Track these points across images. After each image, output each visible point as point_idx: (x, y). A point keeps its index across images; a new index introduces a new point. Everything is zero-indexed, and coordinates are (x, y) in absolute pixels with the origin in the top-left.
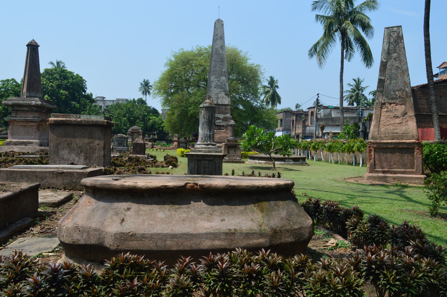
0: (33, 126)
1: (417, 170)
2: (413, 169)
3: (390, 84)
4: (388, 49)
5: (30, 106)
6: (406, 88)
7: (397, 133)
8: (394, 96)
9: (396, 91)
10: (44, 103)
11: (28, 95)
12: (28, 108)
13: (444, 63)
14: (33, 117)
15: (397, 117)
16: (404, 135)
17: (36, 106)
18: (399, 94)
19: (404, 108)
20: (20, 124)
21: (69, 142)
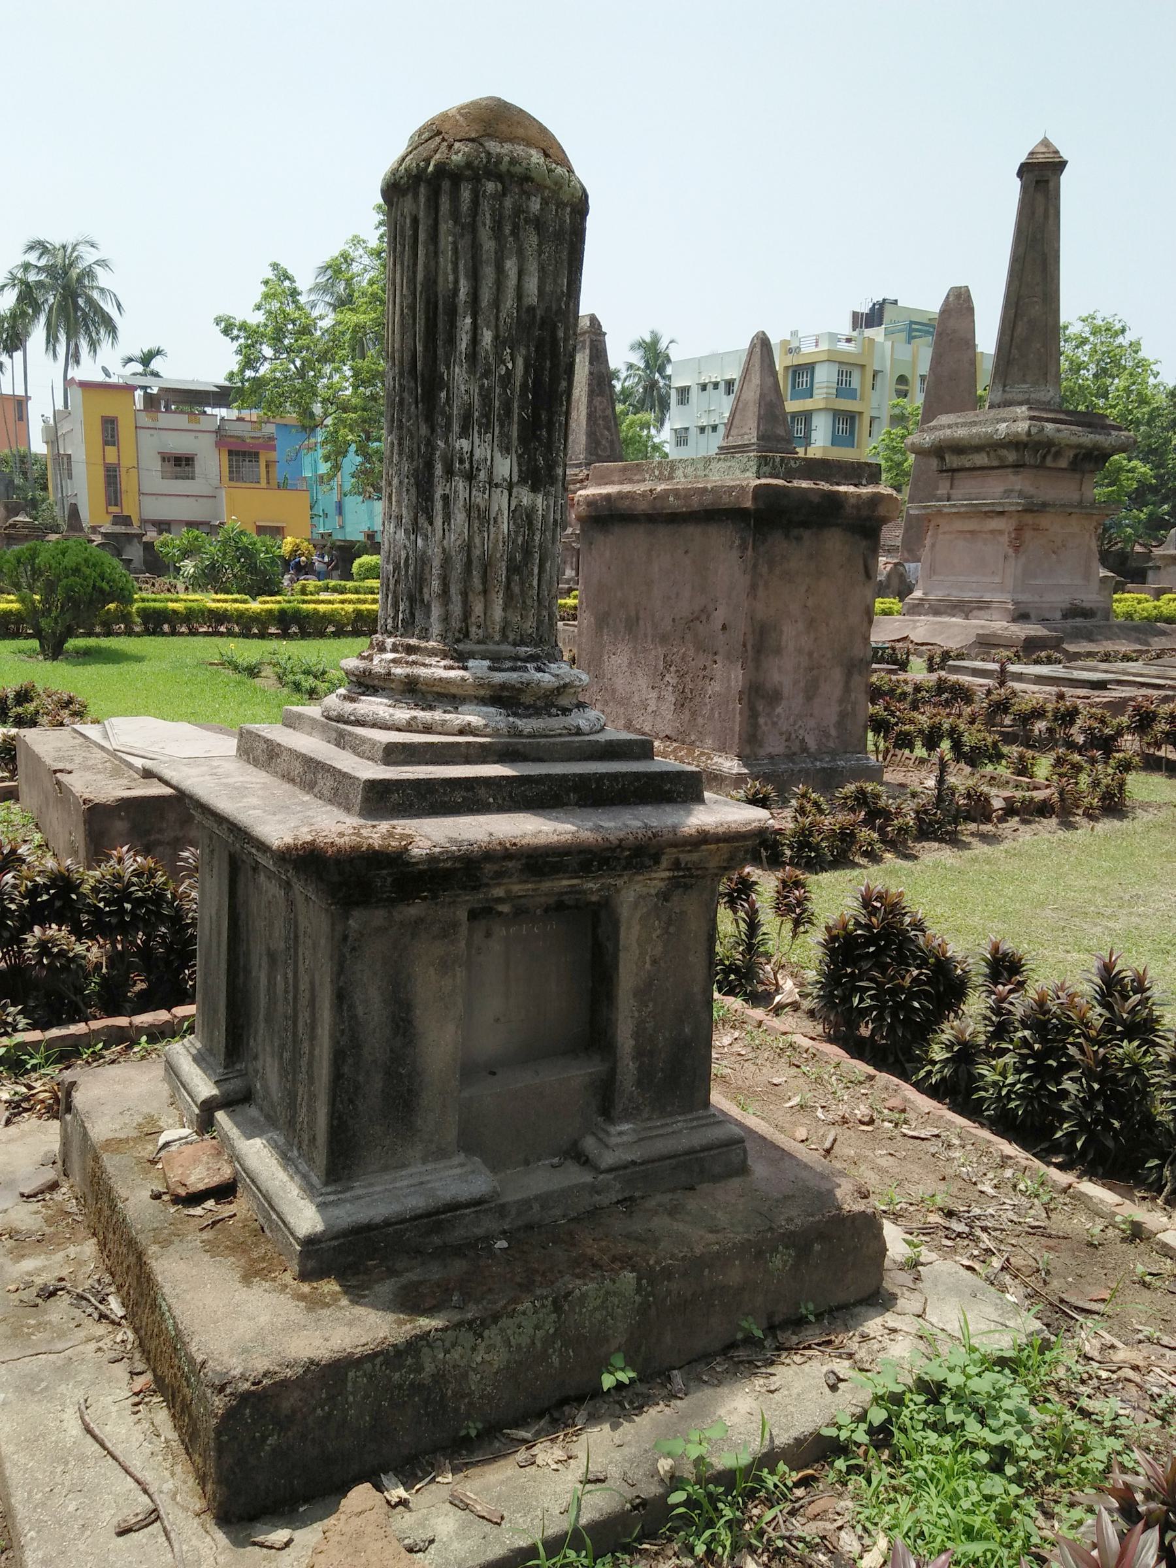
0: (1001, 532)
5: (991, 446)
10: (1049, 426)
11: (998, 397)
12: (988, 453)
14: (1005, 492)
17: (1015, 444)
20: (959, 525)
21: (633, 614)
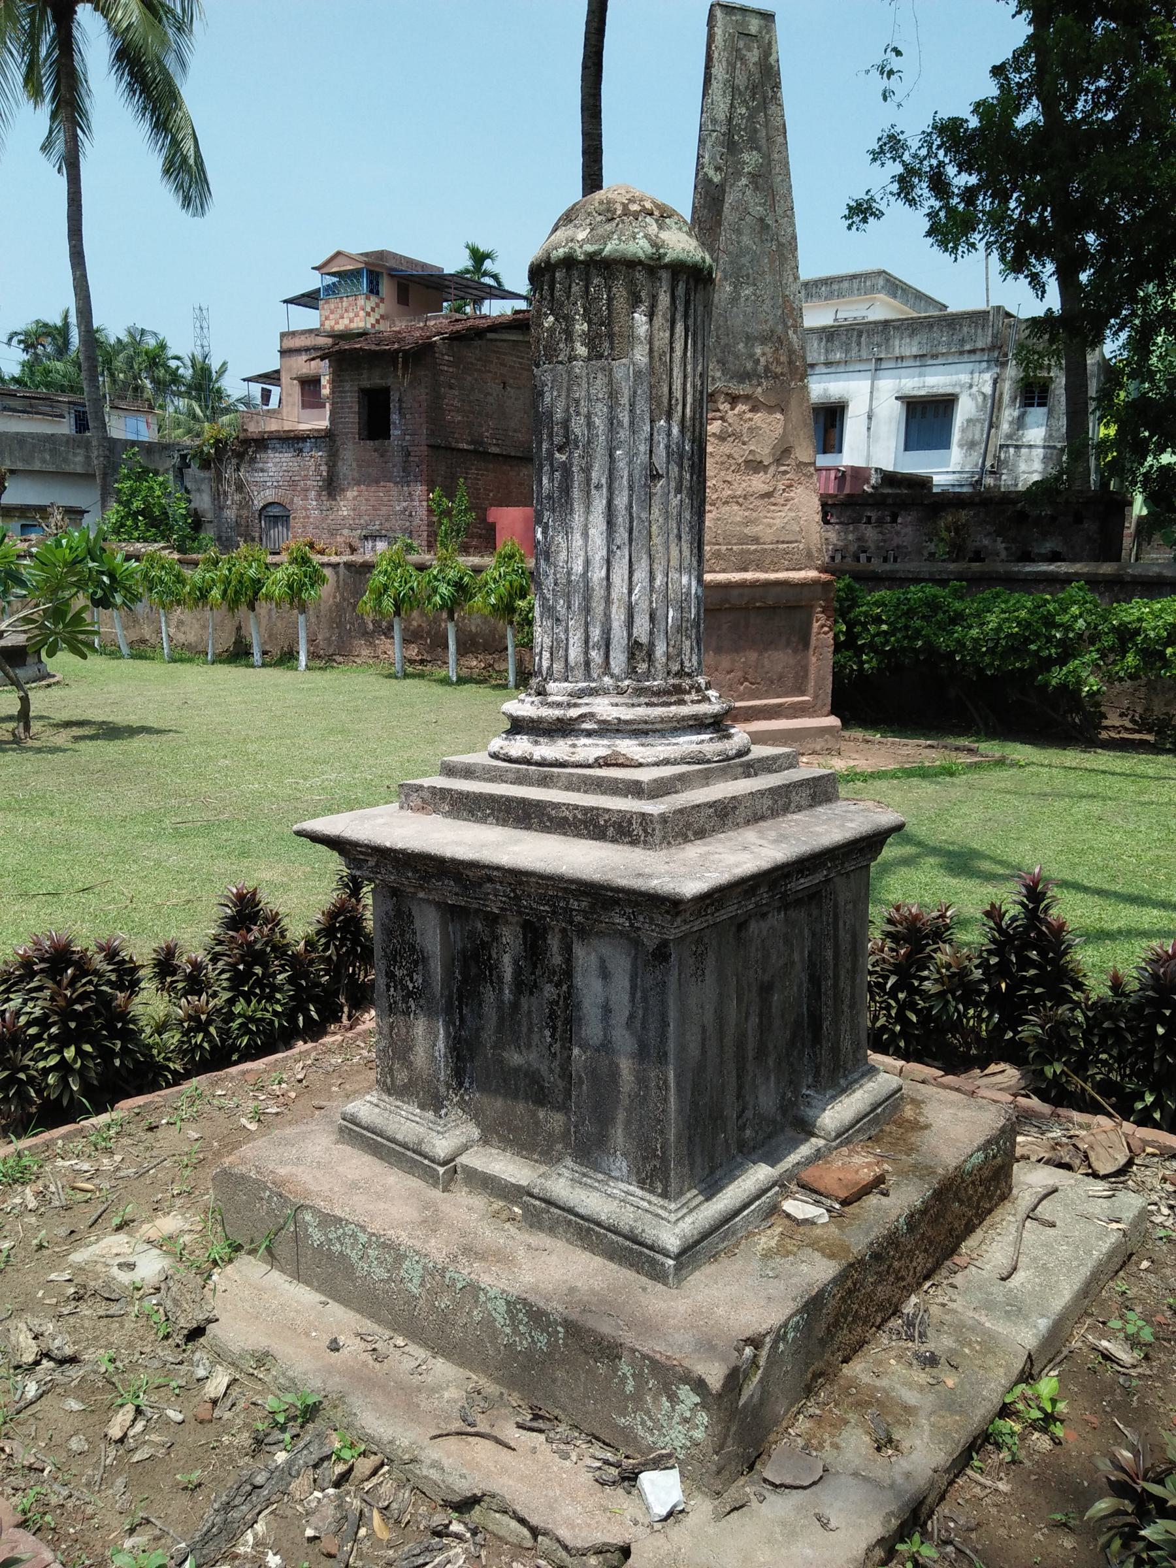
1: (816, 697)
2: (803, 693)
3: (734, 300)
4: (730, 120)
6: (790, 332)
7: (756, 540)
8: (749, 366)
9: (756, 338)
13: (339, 254)
15: (754, 466)
16: (780, 546)
18: (764, 354)
19: (782, 423)
